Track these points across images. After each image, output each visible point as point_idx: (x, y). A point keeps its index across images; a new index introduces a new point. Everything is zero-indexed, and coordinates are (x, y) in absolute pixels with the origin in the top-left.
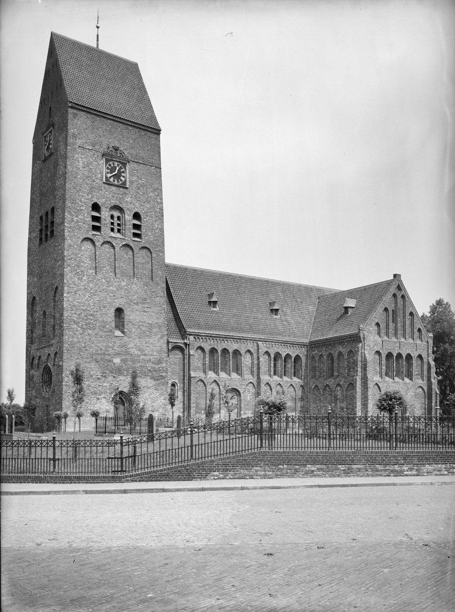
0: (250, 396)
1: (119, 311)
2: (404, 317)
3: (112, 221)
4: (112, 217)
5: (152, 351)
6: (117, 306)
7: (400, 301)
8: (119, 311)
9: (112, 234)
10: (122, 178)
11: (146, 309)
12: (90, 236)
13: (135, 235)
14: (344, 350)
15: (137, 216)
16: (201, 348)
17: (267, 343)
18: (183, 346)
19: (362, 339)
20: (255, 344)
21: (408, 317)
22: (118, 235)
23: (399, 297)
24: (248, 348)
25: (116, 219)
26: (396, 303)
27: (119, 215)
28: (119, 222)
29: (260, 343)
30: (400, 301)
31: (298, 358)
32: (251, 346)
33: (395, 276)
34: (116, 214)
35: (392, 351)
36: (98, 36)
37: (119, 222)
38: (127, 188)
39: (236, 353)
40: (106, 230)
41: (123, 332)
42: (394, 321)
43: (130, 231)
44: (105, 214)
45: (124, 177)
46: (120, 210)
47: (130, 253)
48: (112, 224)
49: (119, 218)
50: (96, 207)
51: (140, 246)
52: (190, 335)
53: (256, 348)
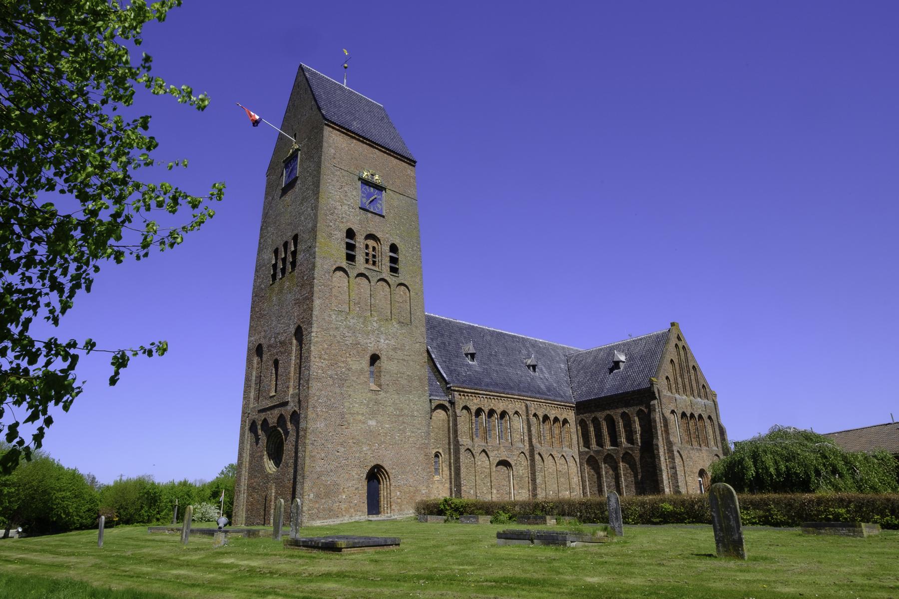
2: (689, 372)
3: (366, 251)
4: (367, 247)
7: (682, 352)
8: (374, 359)
9: (367, 266)
10: (378, 205)
14: (631, 411)
15: (394, 248)
16: (466, 408)
18: (447, 404)
19: (657, 395)
20: (523, 404)
21: (692, 371)
23: (681, 347)
24: (516, 409)
25: (371, 249)
26: (679, 354)
27: (375, 245)
28: (373, 253)
30: (682, 352)
33: (673, 324)
34: (371, 243)
35: (685, 411)
37: (373, 253)
38: (383, 217)
39: (503, 414)
40: (360, 258)
41: (380, 386)
42: (682, 376)
43: (386, 264)
44: (360, 242)
45: (381, 205)
48: (367, 254)
49: (374, 249)
50: (350, 234)
51: (398, 282)
53: (524, 408)
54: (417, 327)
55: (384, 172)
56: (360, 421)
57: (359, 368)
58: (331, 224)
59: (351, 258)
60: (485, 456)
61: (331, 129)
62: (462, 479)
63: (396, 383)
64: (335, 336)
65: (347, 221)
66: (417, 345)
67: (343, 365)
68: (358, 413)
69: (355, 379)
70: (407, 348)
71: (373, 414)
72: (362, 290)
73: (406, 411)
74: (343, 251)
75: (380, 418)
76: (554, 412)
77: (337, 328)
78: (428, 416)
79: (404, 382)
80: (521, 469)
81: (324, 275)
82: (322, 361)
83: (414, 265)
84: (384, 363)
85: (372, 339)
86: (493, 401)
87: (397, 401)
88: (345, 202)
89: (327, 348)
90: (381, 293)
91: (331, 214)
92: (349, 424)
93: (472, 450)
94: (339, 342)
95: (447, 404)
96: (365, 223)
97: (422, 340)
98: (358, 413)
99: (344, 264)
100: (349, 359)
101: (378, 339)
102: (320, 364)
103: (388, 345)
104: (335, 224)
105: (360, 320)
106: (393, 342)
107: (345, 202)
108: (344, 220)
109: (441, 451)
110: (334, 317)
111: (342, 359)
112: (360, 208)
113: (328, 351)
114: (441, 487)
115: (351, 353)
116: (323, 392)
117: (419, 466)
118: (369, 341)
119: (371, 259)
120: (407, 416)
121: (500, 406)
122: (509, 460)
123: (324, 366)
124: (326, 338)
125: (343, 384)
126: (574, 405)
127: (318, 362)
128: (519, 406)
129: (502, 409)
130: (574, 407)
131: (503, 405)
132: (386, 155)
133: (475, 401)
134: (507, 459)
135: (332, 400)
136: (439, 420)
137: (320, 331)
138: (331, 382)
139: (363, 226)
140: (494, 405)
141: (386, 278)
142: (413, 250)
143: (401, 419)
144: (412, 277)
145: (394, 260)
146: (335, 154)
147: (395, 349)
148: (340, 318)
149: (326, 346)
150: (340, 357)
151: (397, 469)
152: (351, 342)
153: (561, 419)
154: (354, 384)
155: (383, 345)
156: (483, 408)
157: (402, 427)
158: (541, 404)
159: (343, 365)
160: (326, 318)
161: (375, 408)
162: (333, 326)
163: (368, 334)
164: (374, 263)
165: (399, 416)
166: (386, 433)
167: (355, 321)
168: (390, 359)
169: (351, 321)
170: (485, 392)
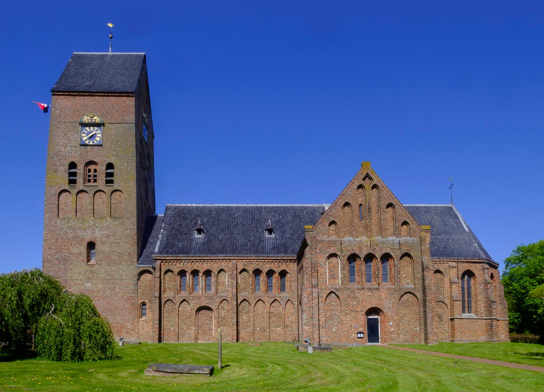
0: (225, 313)
1: (91, 246)
5: (122, 276)
8: (91, 246)
39: (208, 273)
40: (80, 179)
46: (94, 163)
54: (128, 219)
55: (103, 111)
56: (79, 284)
57: (78, 252)
58: (57, 163)
59: (72, 182)
60: (187, 303)
61: (57, 97)
63: (108, 259)
64: (60, 234)
65: (69, 158)
66: (128, 231)
67: (66, 251)
68: (77, 279)
69: (75, 259)
70: (119, 234)
71: (89, 280)
72: (83, 201)
73: (116, 277)
74: (66, 178)
75: (94, 281)
76: (268, 266)
77: (61, 229)
78: (136, 279)
79: (115, 257)
80: (223, 312)
81: (52, 197)
82: (51, 250)
83: (129, 174)
85: (89, 232)
87: (109, 270)
88: (68, 144)
89: (54, 242)
90: (100, 200)
91: (57, 156)
92: (70, 286)
93: (173, 300)
94: (62, 237)
95: (151, 270)
96: (85, 155)
97: (133, 227)
98: (77, 279)
99: (67, 187)
100: (70, 247)
101: (93, 232)
102: (49, 252)
103: (102, 234)
104: (59, 162)
105: (79, 221)
106: (106, 232)
107: (68, 144)
108: (68, 157)
109: (146, 301)
110: (59, 222)
111: (66, 248)
112: (81, 145)
113: (55, 244)
114: (145, 324)
115: (72, 243)
116: (52, 269)
117: (126, 311)
118: (86, 234)
119: (90, 179)
120: (117, 279)
121: (202, 267)
122: (210, 306)
123: (52, 253)
124: (53, 236)
125: (66, 263)
126: (295, 258)
127: (47, 251)
128: (223, 265)
130: (295, 260)
131: (207, 266)
132: (105, 98)
134: (208, 305)
135: (58, 273)
136: (147, 281)
137: (49, 233)
138: (57, 262)
139: (83, 157)
140: (198, 266)
141: (102, 189)
142: (128, 163)
143: (111, 281)
144: (126, 183)
146: (60, 113)
147: (108, 236)
148: (63, 222)
149: (53, 241)
150: (63, 247)
151: (107, 312)
152: (72, 236)
153: (278, 270)
154: (74, 262)
155: (97, 235)
156: (186, 270)
157: (112, 286)
158: (252, 261)
159: (66, 251)
160: (53, 224)
161: (91, 275)
162: (58, 228)
163: (85, 229)
164: (95, 181)
165: (110, 279)
166: (99, 291)
167: (75, 223)
168: (103, 243)
169: (72, 223)
170: (187, 258)
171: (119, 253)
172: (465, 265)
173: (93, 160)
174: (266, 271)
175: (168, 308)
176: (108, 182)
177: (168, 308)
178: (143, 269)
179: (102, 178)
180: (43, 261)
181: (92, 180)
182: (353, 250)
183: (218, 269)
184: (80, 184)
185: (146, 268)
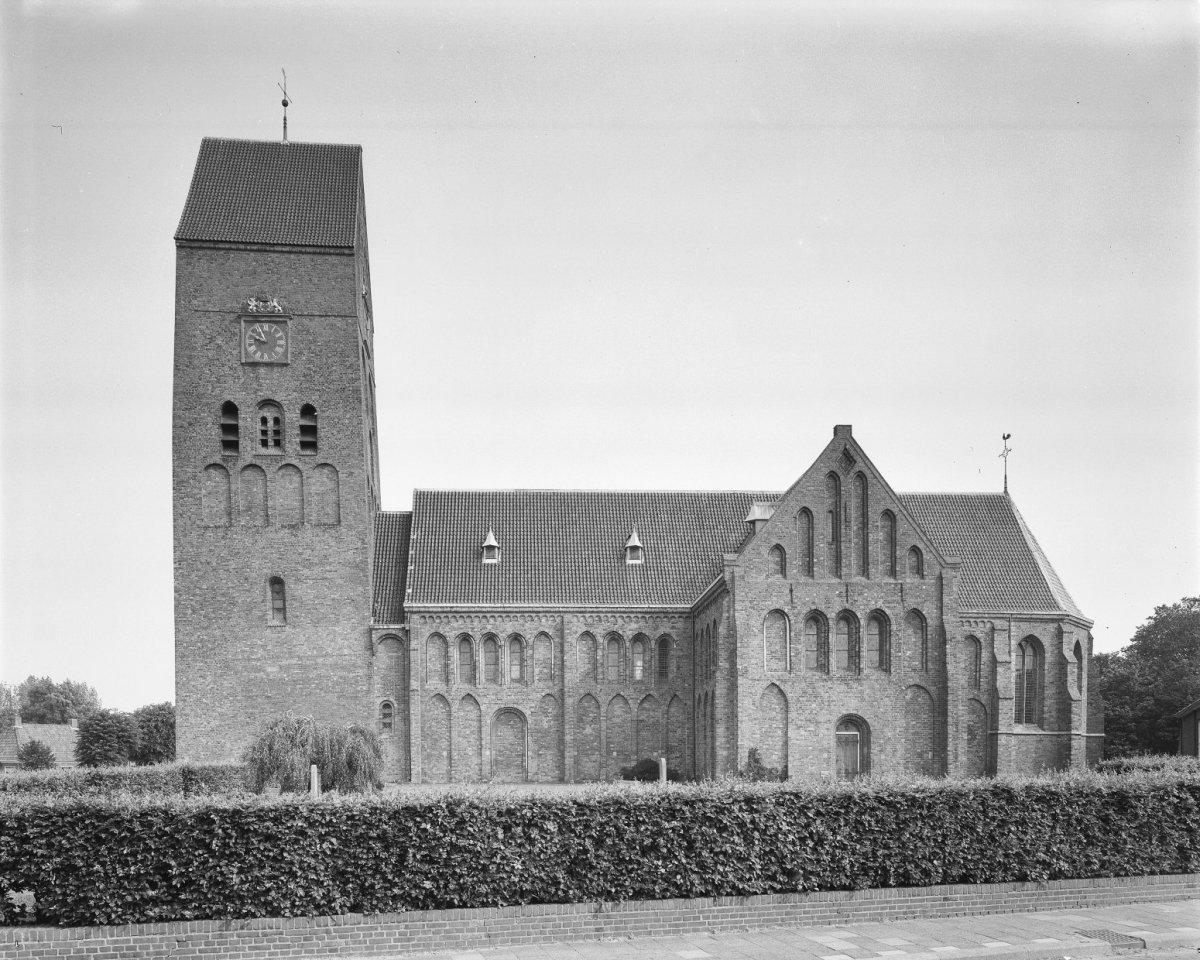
1: (277, 583)
4: (264, 421)
6: (268, 572)
8: (277, 583)
11: (327, 575)
12: (219, 461)
13: (304, 445)
15: (308, 411)
17: (587, 615)
22: (272, 451)
24: (541, 629)
29: (567, 617)
31: (664, 642)
32: (547, 625)
36: (285, 119)
39: (516, 638)
47: (296, 478)
50: (230, 409)
52: (412, 612)
62: (412, 738)
80: (546, 720)
84: (291, 587)
86: (492, 621)
122: (520, 708)
129: (510, 631)
133: (455, 625)
145: (309, 431)
156: (470, 633)
164: (277, 443)
171: (333, 600)
172: (1024, 626)
173: (271, 397)
174: (631, 637)
175: (436, 712)
176: (304, 445)
177: (436, 712)
178: (384, 632)
179: (293, 438)
180: (176, 621)
181: (271, 443)
182: (813, 603)
183: (536, 632)
184: (250, 449)
185: (390, 631)
